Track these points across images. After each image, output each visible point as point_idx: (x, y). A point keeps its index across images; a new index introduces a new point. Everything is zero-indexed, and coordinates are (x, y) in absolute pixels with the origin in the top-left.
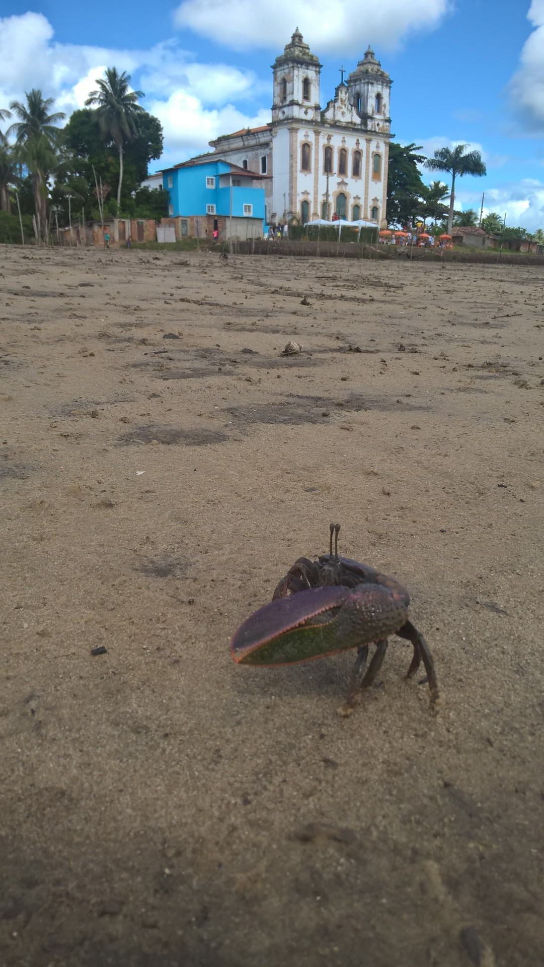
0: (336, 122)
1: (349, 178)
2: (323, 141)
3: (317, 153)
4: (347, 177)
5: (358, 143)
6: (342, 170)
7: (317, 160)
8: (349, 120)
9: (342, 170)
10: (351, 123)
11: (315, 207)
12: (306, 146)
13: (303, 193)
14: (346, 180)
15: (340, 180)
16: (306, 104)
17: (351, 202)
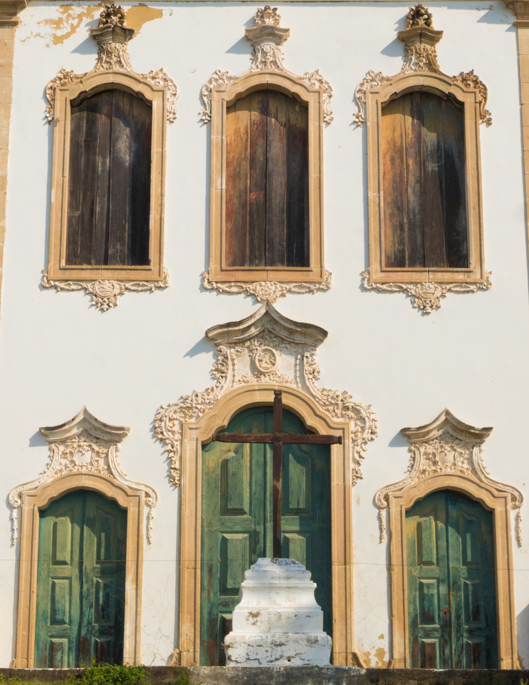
4: (321, 284)
5: (416, 34)
14: (294, 307)
15: (238, 308)
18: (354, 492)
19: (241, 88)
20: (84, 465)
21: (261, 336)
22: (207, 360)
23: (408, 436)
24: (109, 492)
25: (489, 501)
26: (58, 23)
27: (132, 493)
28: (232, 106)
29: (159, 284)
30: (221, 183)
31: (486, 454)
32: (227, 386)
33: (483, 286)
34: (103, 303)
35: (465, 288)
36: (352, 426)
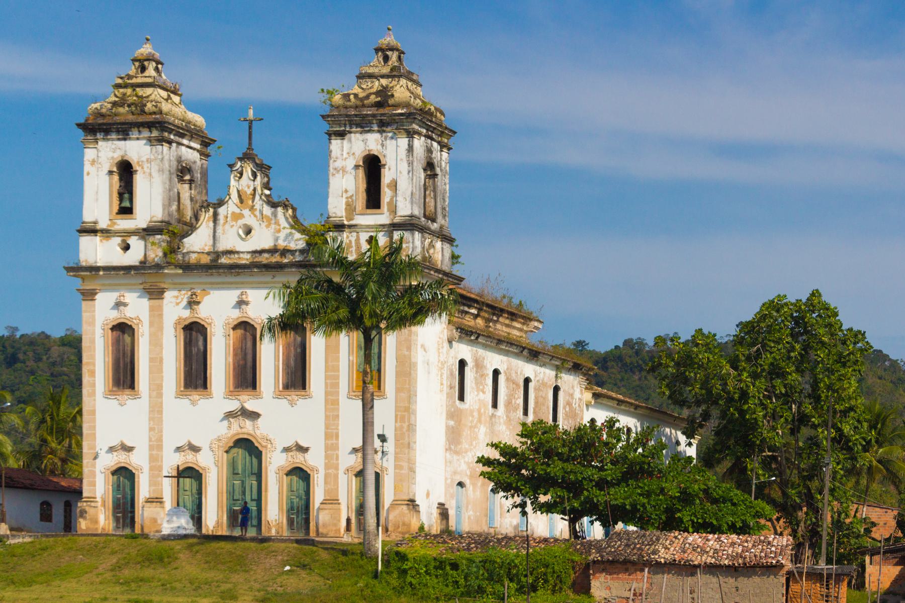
0: (217, 255)
1: (268, 397)
2: (174, 308)
3: (156, 342)
4: (259, 396)
6: (246, 377)
7: (157, 362)
8: (268, 244)
9: (246, 377)
10: (273, 251)
11: (154, 482)
12: (123, 330)
13: (111, 449)
15: (234, 405)
16: (125, 224)
17: (275, 463)
18: (269, 468)
19: (236, 323)
20: (188, 459)
21: (241, 415)
22: (226, 423)
23: (287, 450)
24: (197, 468)
25: (309, 472)
26: (177, 297)
27: (204, 469)
28: (234, 328)
29: (210, 395)
30: (231, 360)
31: (308, 456)
32: (232, 432)
33: (309, 396)
34: (194, 403)
35: (305, 397)
36: (269, 446)
